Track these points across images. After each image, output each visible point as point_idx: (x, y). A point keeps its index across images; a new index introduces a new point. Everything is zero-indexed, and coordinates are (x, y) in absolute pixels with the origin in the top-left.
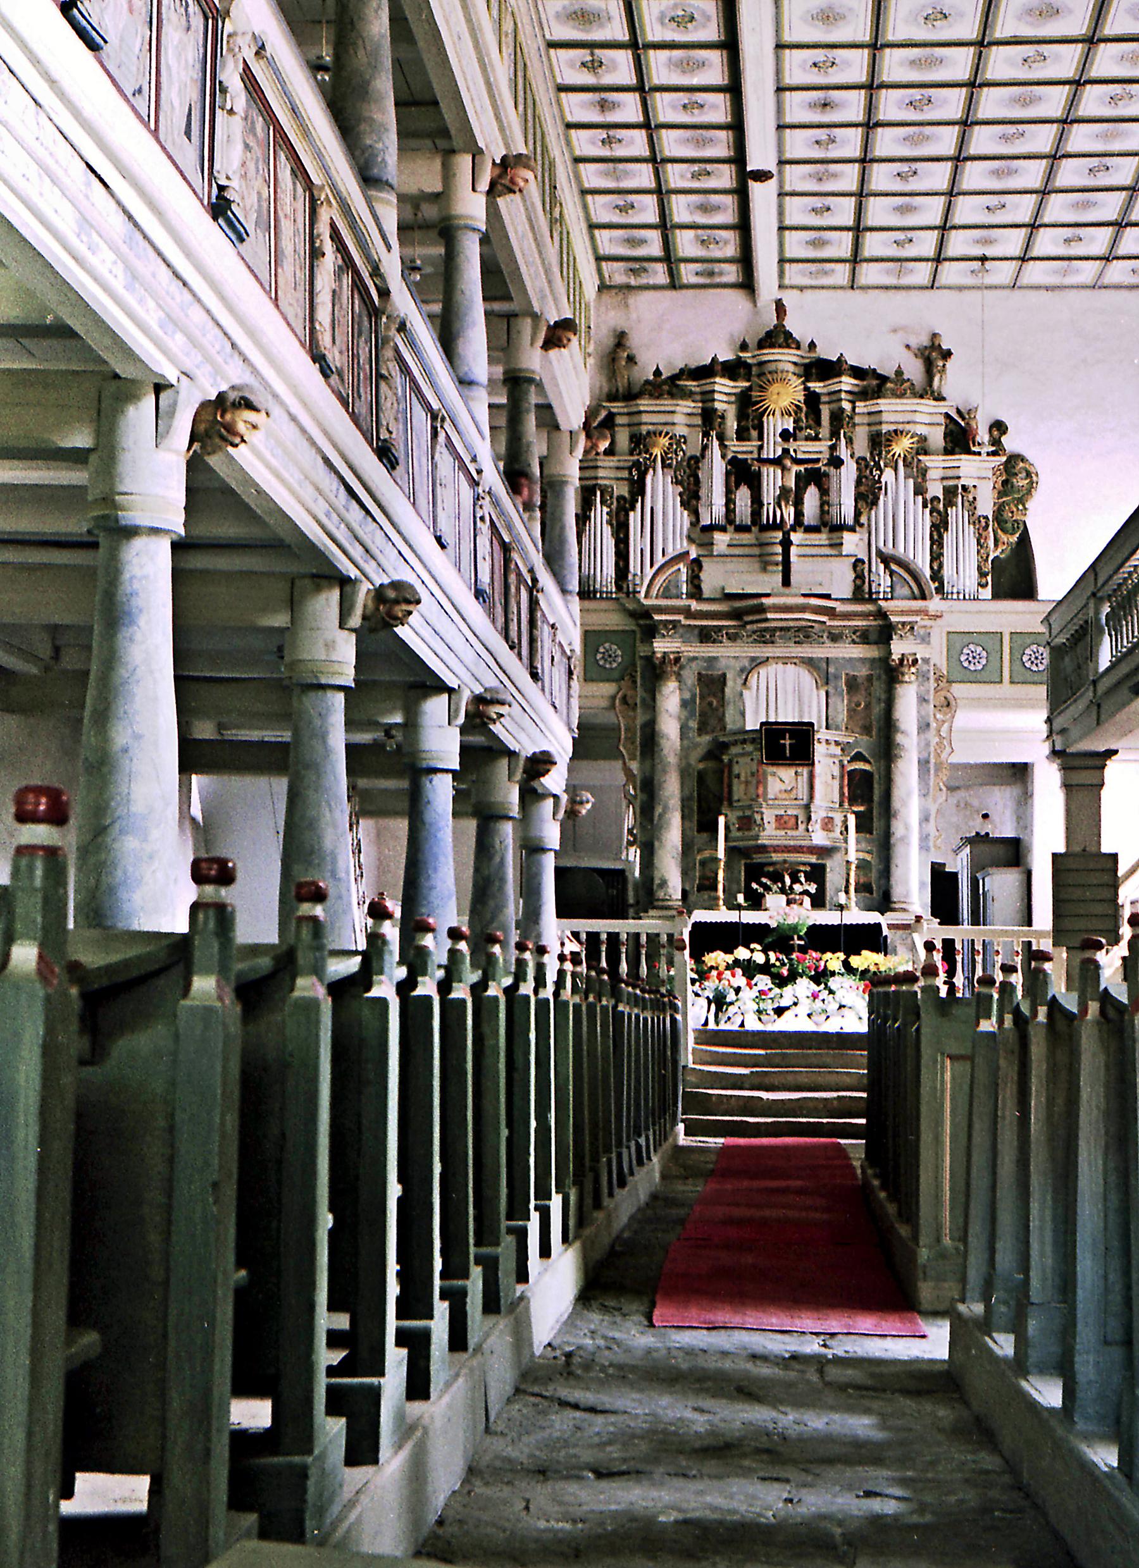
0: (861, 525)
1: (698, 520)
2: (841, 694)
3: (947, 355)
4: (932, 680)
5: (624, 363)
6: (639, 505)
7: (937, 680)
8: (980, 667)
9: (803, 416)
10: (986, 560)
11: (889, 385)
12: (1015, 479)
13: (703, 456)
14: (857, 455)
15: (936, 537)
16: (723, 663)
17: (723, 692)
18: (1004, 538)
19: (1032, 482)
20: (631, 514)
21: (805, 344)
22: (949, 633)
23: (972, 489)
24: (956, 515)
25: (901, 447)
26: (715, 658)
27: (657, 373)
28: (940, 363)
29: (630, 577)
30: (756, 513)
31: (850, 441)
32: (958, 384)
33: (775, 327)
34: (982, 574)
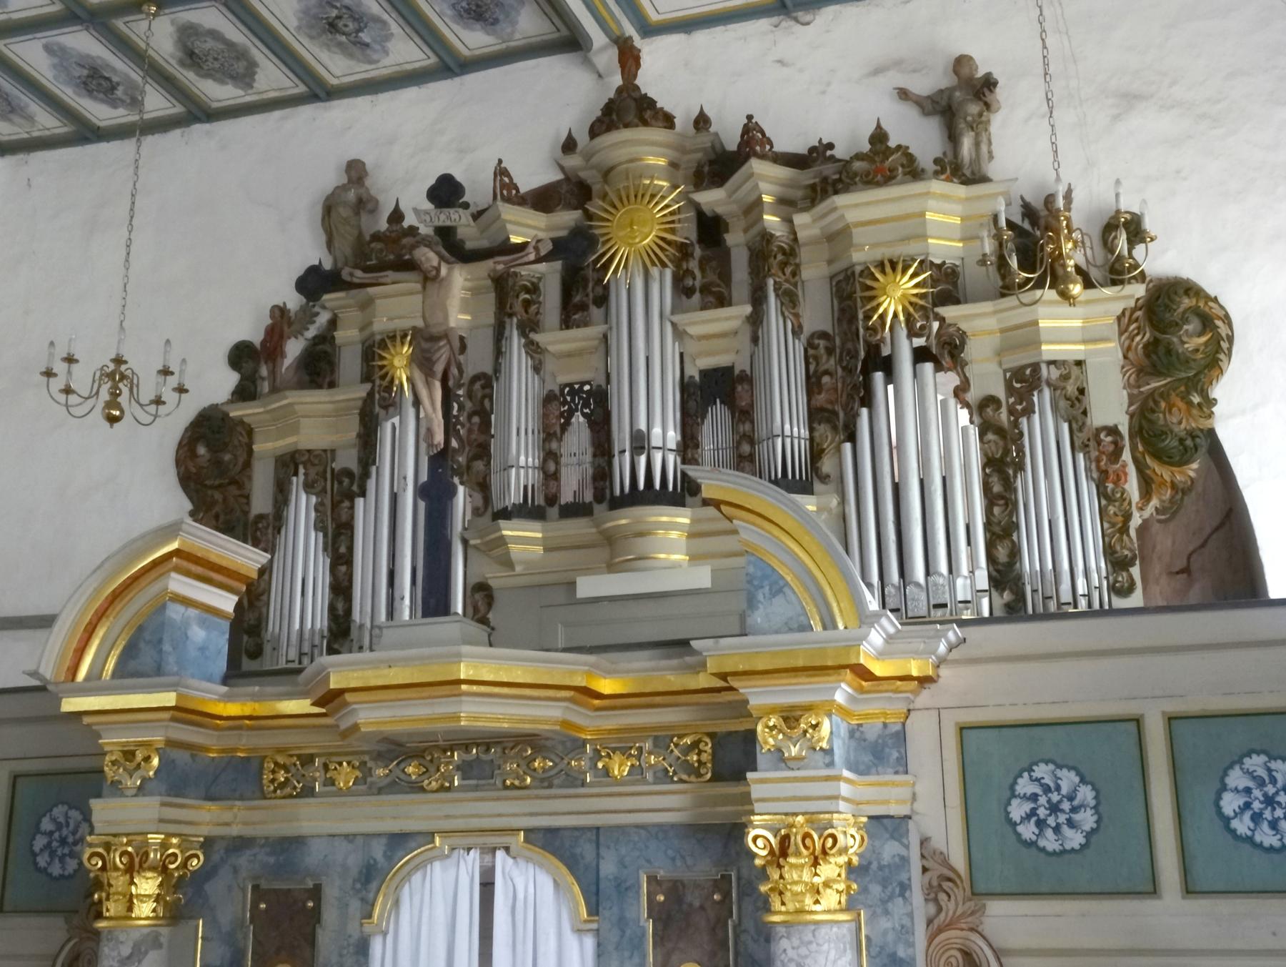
0: (824, 479)
1: (487, 499)
2: (637, 945)
3: (983, 88)
4: (917, 896)
5: (344, 212)
6: (371, 485)
7: (933, 893)
8: (1074, 839)
9: (693, 265)
10: (1124, 529)
12: (1178, 337)
13: (497, 370)
14: (808, 329)
15: (997, 488)
16: (314, 855)
17: (312, 941)
18: (1163, 472)
19: (1217, 339)
20: (360, 502)
22: (962, 729)
23: (1075, 371)
24: (1044, 431)
25: (895, 296)
26: (297, 842)
27: (397, 216)
28: (974, 108)
29: (354, 633)
30: (602, 475)
31: (790, 299)
32: (1020, 150)
33: (619, 91)
34: (1117, 563)
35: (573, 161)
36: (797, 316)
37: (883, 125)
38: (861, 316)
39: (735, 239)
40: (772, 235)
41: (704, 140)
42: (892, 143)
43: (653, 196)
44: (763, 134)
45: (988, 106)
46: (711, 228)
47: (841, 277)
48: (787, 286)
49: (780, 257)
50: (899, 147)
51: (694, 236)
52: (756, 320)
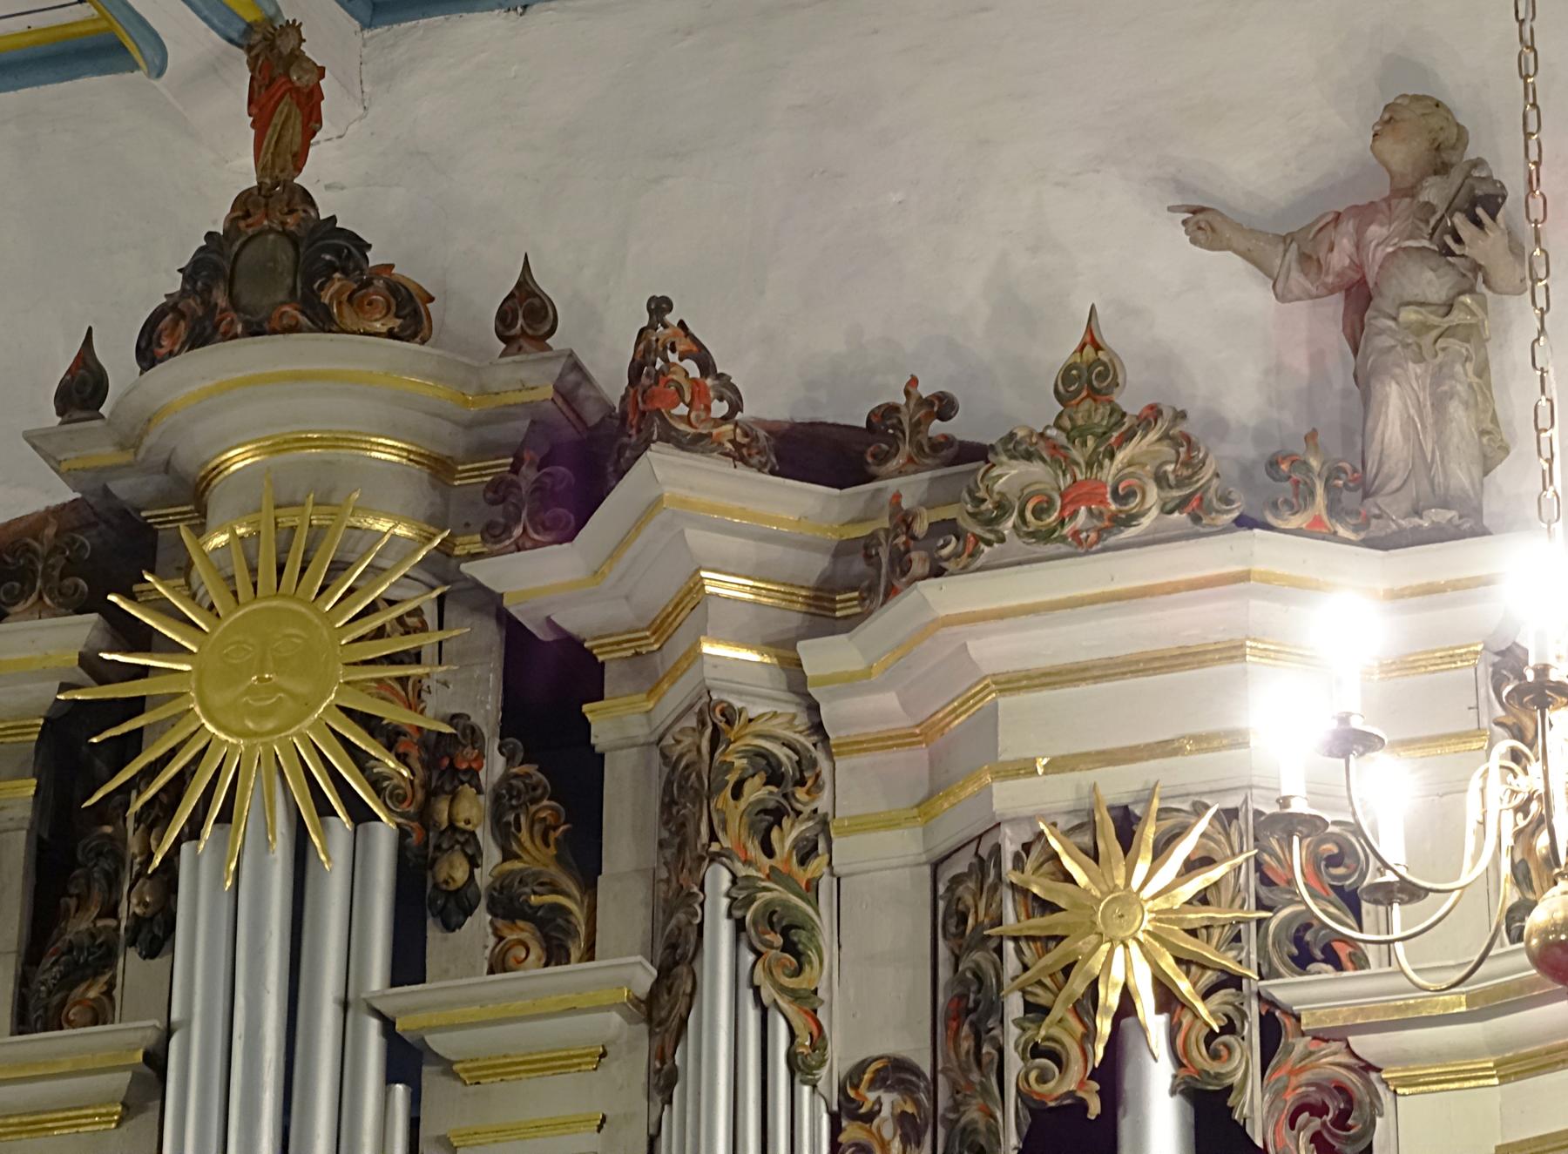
9: (472, 810)
11: (1010, 475)
21: (471, 298)
33: (245, 204)
35: (95, 446)
36: (807, 1000)
37: (1108, 337)
38: (1014, 1006)
39: (613, 723)
40: (730, 715)
41: (528, 381)
42: (1130, 401)
43: (339, 568)
44: (706, 365)
45: (1474, 275)
46: (551, 684)
47: (961, 865)
48: (778, 893)
49: (757, 791)
50: (1155, 412)
51: (486, 711)
52: (666, 1010)
